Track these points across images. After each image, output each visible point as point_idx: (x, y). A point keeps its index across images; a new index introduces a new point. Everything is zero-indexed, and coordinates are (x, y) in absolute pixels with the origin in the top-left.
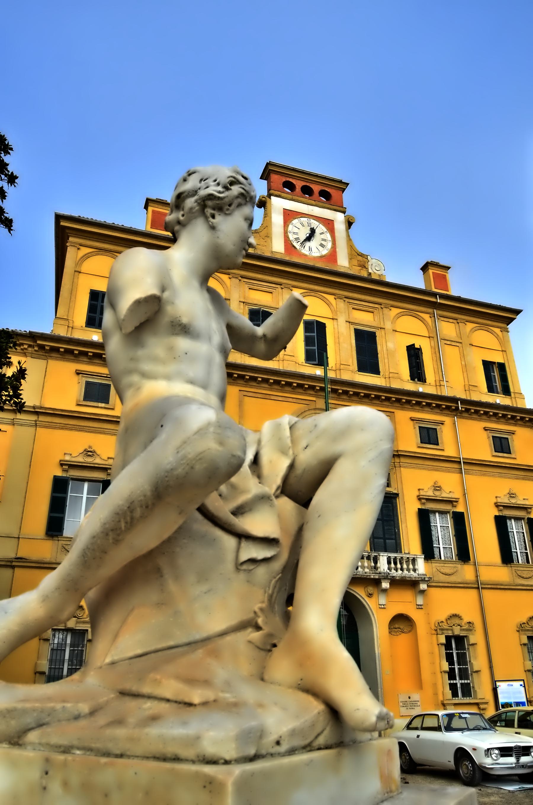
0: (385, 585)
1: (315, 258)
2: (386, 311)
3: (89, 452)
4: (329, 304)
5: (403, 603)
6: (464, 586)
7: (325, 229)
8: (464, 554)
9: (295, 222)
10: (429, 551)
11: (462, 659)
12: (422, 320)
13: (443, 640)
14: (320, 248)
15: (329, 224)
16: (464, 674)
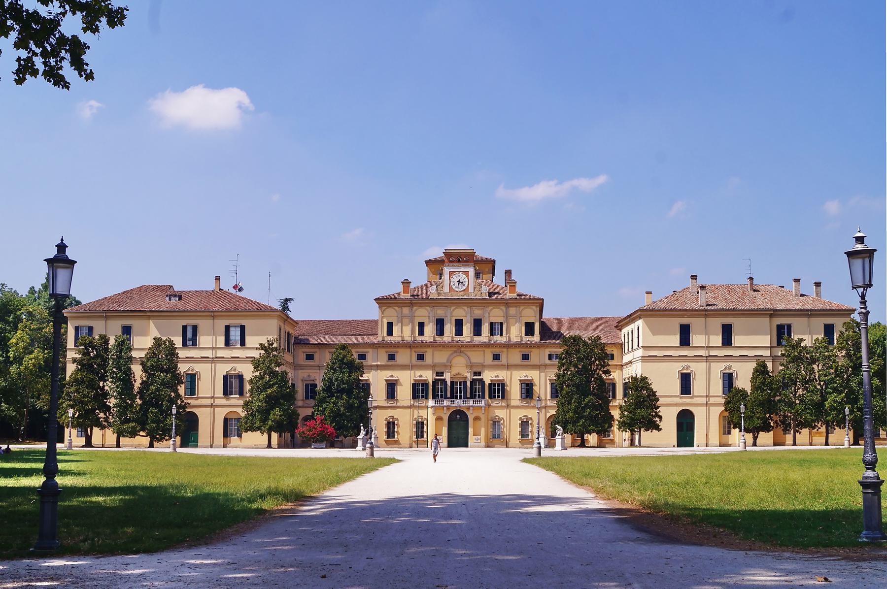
6: (502, 407)
8: (503, 398)
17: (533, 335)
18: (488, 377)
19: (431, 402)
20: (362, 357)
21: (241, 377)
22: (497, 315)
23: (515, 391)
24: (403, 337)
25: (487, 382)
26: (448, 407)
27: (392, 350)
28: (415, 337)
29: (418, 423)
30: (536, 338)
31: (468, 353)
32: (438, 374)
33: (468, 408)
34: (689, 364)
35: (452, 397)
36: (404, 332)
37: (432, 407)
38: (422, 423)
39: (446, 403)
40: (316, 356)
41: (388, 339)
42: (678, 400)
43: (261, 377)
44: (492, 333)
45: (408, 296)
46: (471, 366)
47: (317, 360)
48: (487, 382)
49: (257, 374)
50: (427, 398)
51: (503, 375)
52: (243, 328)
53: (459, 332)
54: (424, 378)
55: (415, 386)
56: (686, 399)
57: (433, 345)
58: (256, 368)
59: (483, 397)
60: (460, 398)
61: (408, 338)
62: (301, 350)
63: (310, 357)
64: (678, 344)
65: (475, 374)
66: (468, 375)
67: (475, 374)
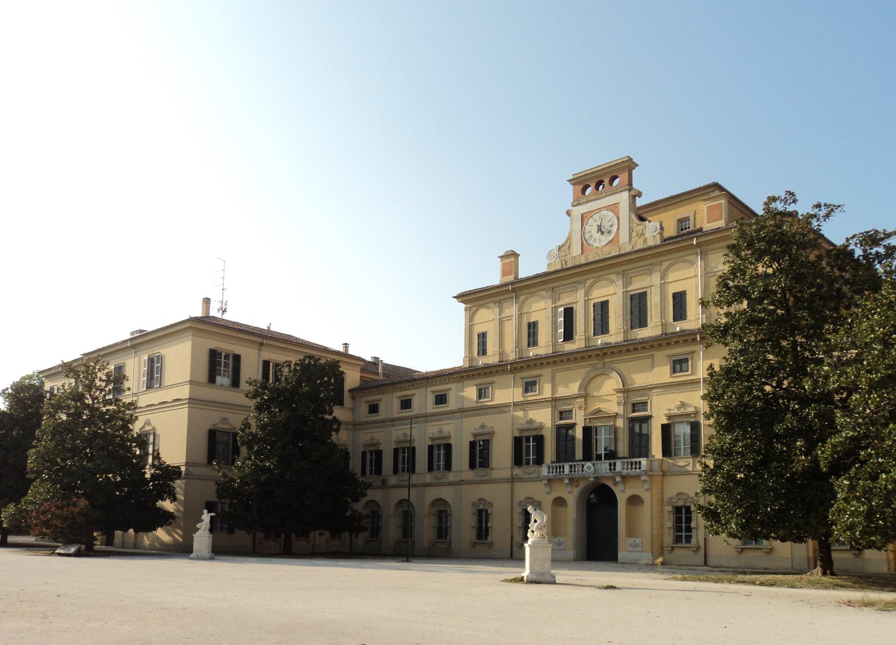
3: (483, 426)
10: (667, 451)
11: (689, 520)
13: (670, 508)
16: (689, 529)
28: (521, 351)
31: (621, 367)
32: (562, 415)
35: (587, 457)
46: (626, 391)
50: (539, 461)
55: (518, 442)
57: (556, 360)
66: (620, 410)
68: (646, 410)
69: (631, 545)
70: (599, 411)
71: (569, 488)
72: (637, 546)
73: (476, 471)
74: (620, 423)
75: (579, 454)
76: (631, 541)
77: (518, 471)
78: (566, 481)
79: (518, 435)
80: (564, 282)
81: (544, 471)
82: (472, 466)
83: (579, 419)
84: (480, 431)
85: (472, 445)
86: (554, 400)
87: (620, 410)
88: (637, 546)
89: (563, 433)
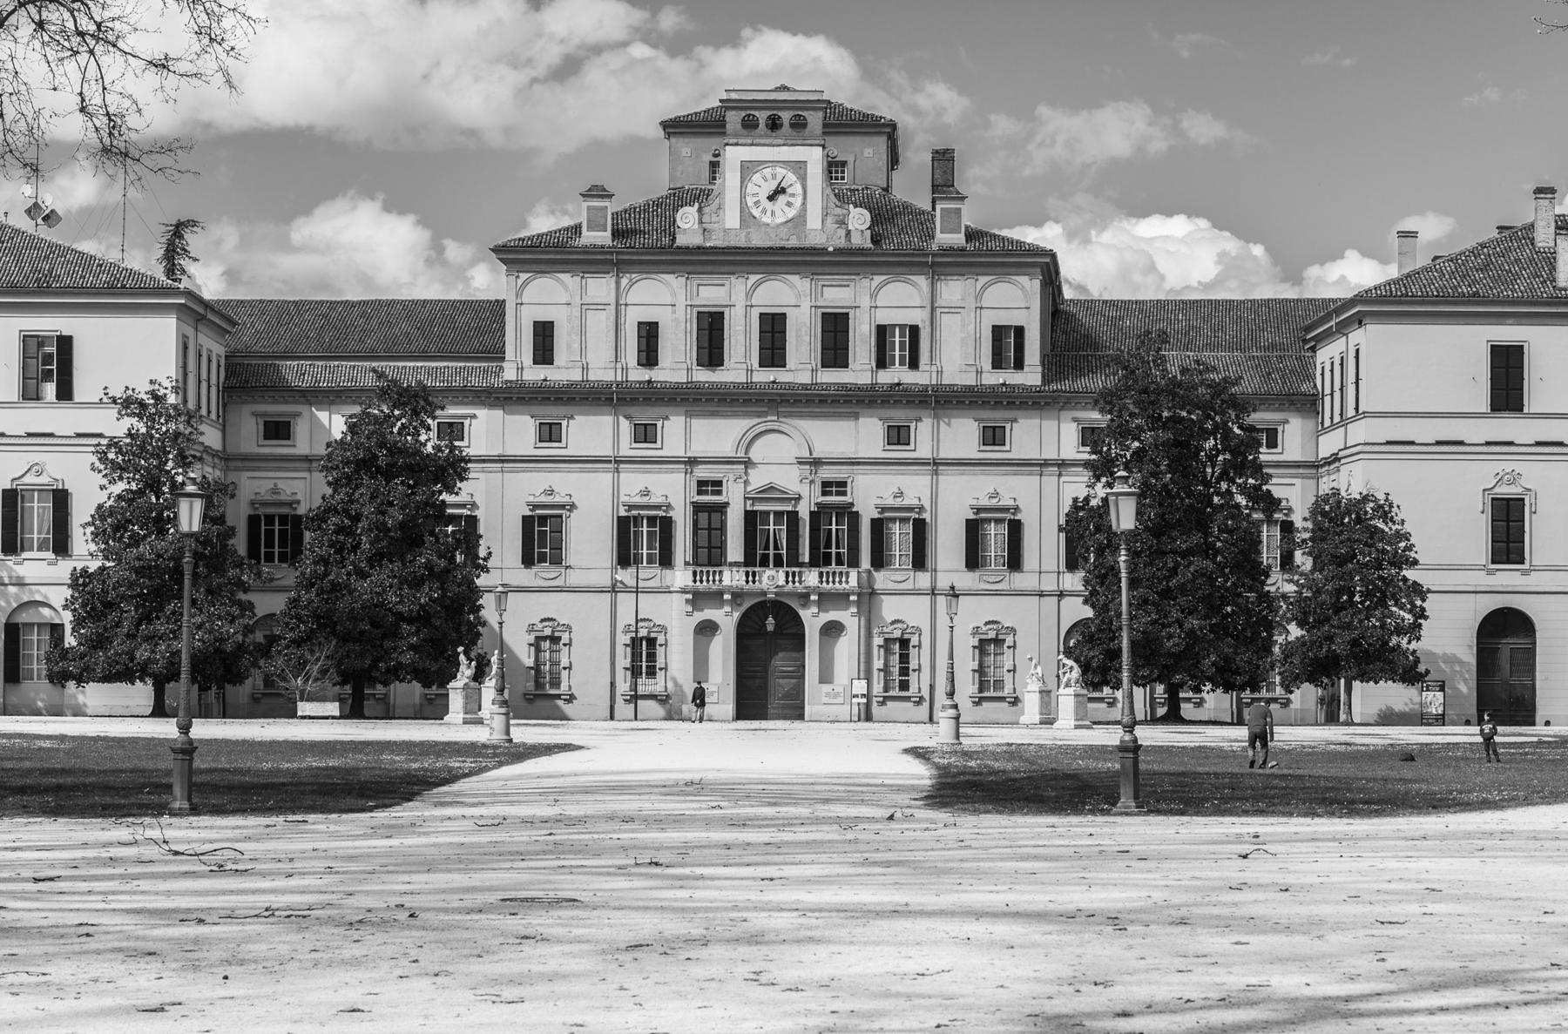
0: (814, 597)
1: (778, 226)
2: (865, 283)
3: (551, 492)
4: (793, 286)
5: (833, 615)
7: (794, 178)
8: (919, 562)
9: (757, 178)
10: (879, 561)
11: (904, 658)
12: (914, 284)
14: (786, 209)
15: (799, 168)
16: (904, 671)
17: (1019, 364)
18: (870, 494)
19: (681, 576)
20: (453, 431)
21: (61, 499)
22: (896, 300)
23: (948, 545)
24: (585, 368)
25: (867, 513)
26: (738, 596)
27: (552, 412)
28: (625, 369)
29: (635, 643)
30: (1031, 376)
32: (702, 486)
33: (804, 598)
34: (1519, 467)
36: (591, 353)
37: (684, 591)
38: (652, 642)
39: (732, 578)
40: (301, 429)
41: (536, 374)
42: (1481, 580)
43: (127, 498)
44: (882, 362)
45: (603, 238)
47: (302, 443)
48: (867, 513)
49: (120, 487)
50: (666, 561)
51: (914, 488)
52: (65, 343)
53: (773, 353)
54: (656, 499)
55: (625, 528)
56: (1507, 577)
58: (117, 470)
59: (854, 562)
60: (778, 563)
61: (601, 372)
62: (247, 409)
63: (278, 430)
64: (1484, 406)
65: (827, 487)
66: (804, 490)
67: (827, 487)
68: (844, 494)
69: (828, 695)
70: (772, 489)
71: (727, 608)
72: (836, 695)
73: (534, 569)
74: (804, 511)
75: (735, 551)
76: (826, 688)
77: (626, 576)
78: (727, 597)
79: (623, 513)
80: (717, 268)
81: (681, 576)
82: (528, 560)
83: (735, 499)
84: (544, 499)
85: (527, 522)
86: (692, 462)
87: (804, 490)
88: (836, 695)
89: (709, 516)
